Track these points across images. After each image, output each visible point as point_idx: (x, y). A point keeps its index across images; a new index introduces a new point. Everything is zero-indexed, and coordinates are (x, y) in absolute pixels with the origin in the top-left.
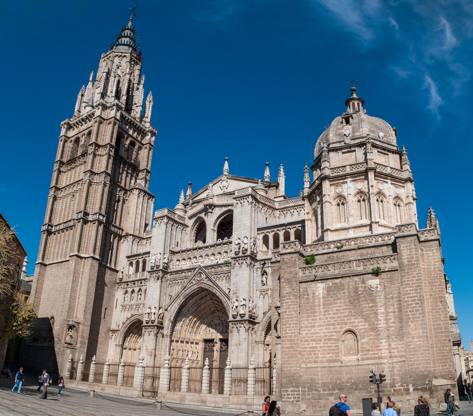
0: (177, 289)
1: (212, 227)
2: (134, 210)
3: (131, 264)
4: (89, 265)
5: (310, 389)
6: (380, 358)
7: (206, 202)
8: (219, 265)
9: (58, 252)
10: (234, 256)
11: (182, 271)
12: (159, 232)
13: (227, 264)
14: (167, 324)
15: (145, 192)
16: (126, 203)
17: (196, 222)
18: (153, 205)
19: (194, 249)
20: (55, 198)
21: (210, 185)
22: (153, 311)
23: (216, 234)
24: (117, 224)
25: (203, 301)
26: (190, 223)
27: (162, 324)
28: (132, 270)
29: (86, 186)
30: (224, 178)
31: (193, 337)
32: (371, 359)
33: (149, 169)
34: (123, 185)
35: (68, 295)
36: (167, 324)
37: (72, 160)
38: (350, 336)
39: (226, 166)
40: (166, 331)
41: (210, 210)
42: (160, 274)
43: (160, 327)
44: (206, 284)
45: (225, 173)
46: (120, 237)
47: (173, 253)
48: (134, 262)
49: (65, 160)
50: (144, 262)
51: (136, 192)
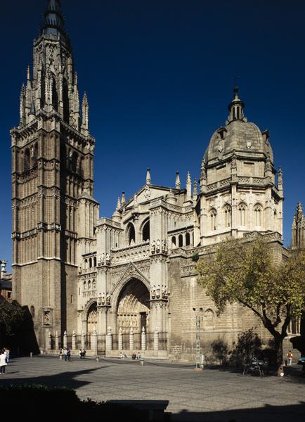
0: (116, 279)
1: (139, 231)
2: (84, 218)
3: (86, 261)
4: (53, 266)
5: (187, 347)
6: (226, 328)
7: (133, 211)
8: (143, 261)
9: (28, 256)
10: (151, 254)
11: (120, 266)
12: (101, 236)
13: (148, 260)
14: (113, 304)
15: (91, 201)
16: (77, 211)
17: (128, 226)
18: (98, 211)
19: (128, 249)
20: (18, 209)
21: (135, 196)
22: (103, 296)
23: (142, 236)
24: (72, 230)
25: (136, 286)
26: (124, 227)
27: (109, 304)
28: (88, 264)
29: (41, 199)
30: (147, 187)
31: (131, 311)
32: (221, 328)
33: (92, 178)
34: (72, 195)
35: (41, 290)
36: (113, 304)
37: (26, 173)
38: (210, 312)
39: (148, 177)
40: (113, 309)
41: (136, 218)
42: (105, 269)
43: (109, 307)
44: (136, 275)
45: (148, 183)
46: (76, 240)
47: (113, 252)
48: (88, 259)
49: (20, 172)
50: (95, 259)
51: (83, 202)
